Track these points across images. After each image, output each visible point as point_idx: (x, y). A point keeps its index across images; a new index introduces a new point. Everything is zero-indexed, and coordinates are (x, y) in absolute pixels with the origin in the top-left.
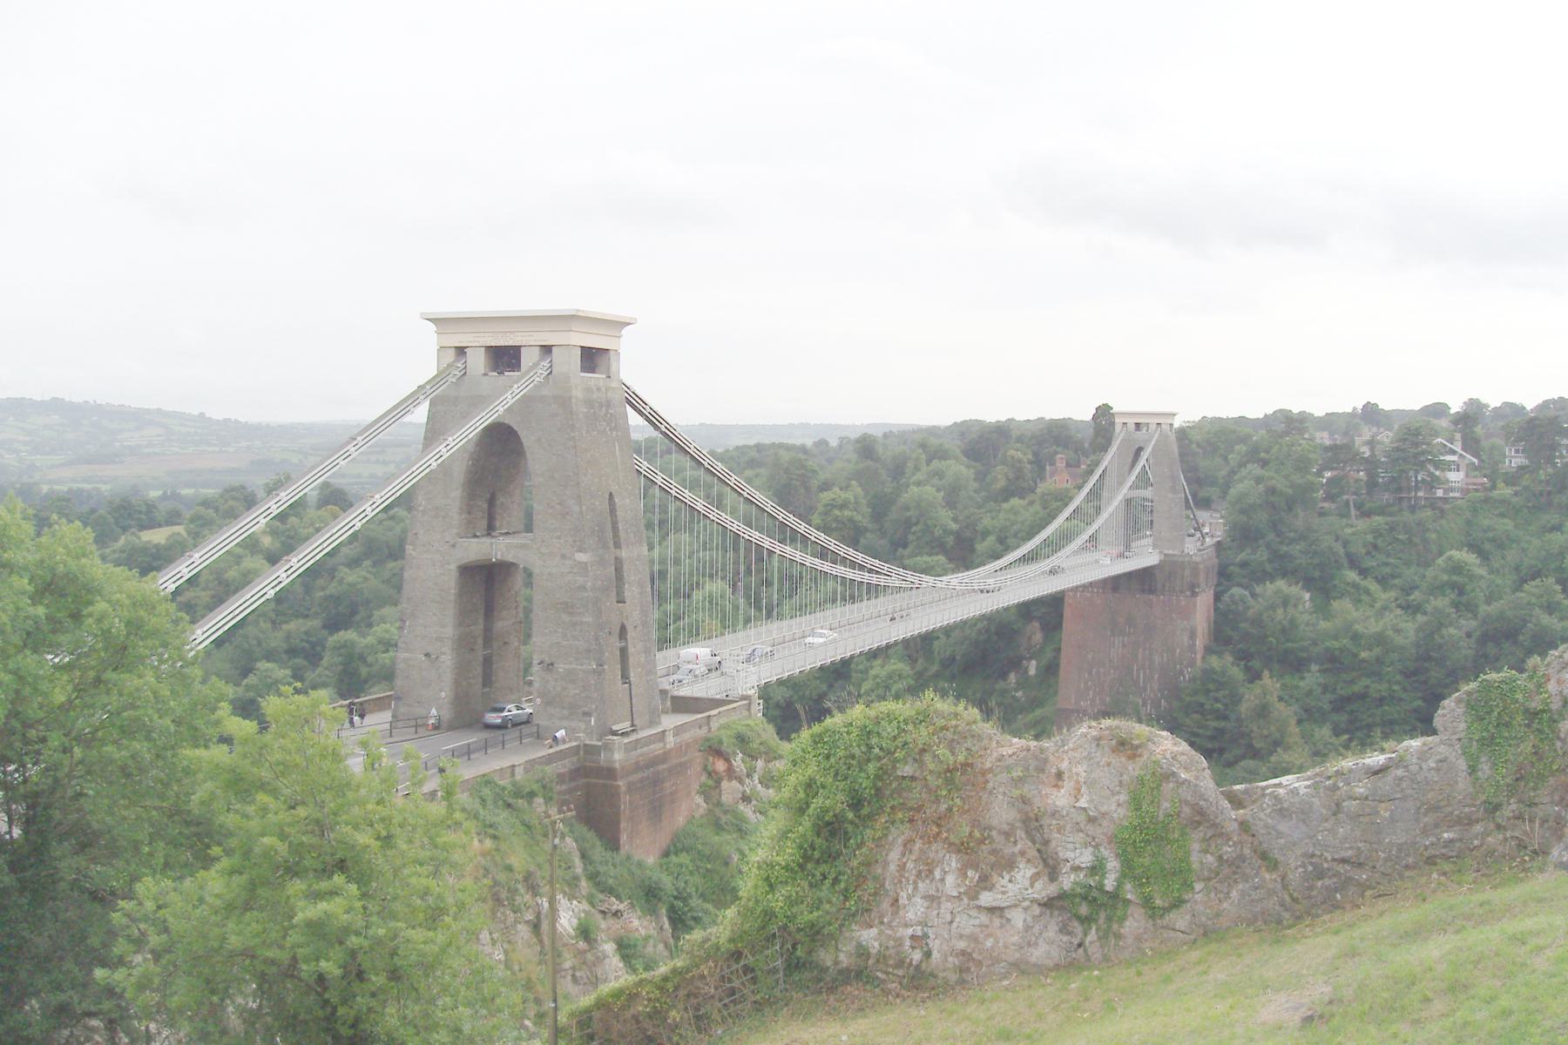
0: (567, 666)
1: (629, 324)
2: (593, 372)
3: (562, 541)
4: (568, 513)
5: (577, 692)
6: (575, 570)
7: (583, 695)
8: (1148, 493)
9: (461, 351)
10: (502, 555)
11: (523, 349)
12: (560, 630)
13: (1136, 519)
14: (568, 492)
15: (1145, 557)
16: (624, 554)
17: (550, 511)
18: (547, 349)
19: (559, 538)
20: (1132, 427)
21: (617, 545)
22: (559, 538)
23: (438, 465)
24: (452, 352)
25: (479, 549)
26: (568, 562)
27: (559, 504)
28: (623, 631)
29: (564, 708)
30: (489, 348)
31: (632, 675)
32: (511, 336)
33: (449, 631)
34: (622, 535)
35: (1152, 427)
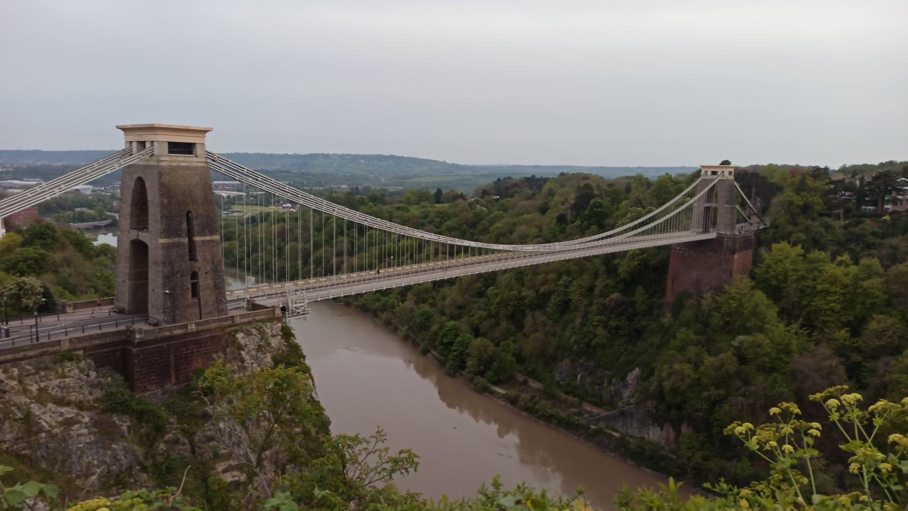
1: (207, 131)
2: (192, 154)
8: (713, 205)
9: (131, 142)
13: (710, 219)
15: (712, 235)
16: (197, 239)
18: (152, 142)
20: (709, 173)
21: (190, 234)
24: (128, 145)
25: (134, 235)
28: (194, 275)
30: (138, 142)
33: (127, 271)
34: (196, 229)
35: (719, 173)
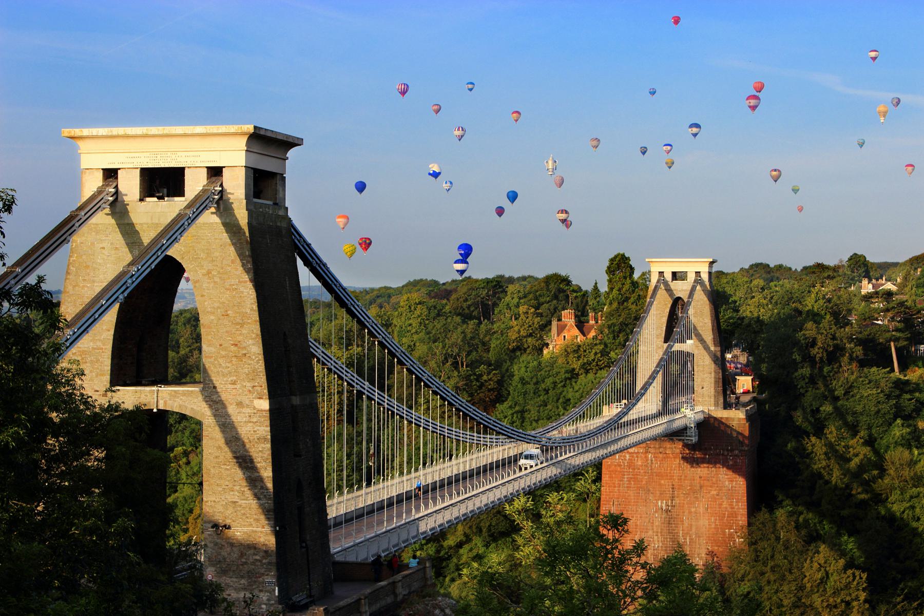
0: (245, 529)
3: (238, 386)
4: (245, 355)
5: (258, 558)
6: (255, 420)
7: (264, 561)
10: (165, 403)
11: (187, 171)
12: (237, 488)
14: (244, 332)
17: (223, 353)
19: (234, 383)
20: (668, 277)
22: (234, 383)
23: (125, 298)
26: (248, 410)
27: (236, 345)
29: (242, 577)
31: (308, 538)
32: (173, 156)
